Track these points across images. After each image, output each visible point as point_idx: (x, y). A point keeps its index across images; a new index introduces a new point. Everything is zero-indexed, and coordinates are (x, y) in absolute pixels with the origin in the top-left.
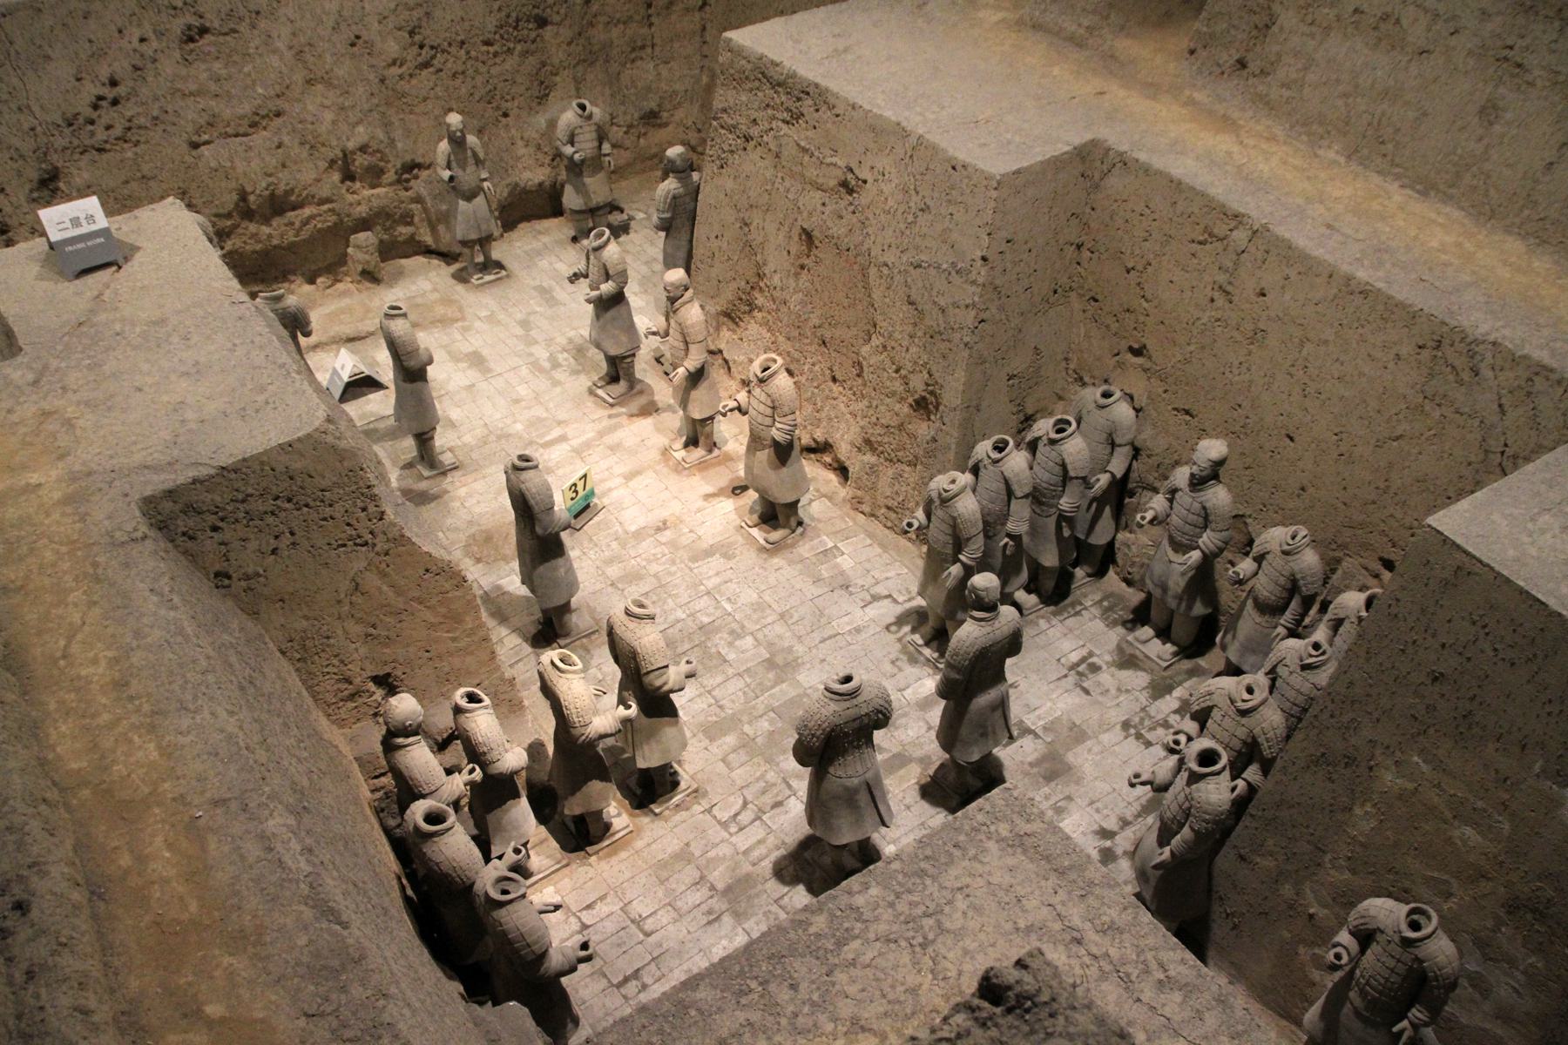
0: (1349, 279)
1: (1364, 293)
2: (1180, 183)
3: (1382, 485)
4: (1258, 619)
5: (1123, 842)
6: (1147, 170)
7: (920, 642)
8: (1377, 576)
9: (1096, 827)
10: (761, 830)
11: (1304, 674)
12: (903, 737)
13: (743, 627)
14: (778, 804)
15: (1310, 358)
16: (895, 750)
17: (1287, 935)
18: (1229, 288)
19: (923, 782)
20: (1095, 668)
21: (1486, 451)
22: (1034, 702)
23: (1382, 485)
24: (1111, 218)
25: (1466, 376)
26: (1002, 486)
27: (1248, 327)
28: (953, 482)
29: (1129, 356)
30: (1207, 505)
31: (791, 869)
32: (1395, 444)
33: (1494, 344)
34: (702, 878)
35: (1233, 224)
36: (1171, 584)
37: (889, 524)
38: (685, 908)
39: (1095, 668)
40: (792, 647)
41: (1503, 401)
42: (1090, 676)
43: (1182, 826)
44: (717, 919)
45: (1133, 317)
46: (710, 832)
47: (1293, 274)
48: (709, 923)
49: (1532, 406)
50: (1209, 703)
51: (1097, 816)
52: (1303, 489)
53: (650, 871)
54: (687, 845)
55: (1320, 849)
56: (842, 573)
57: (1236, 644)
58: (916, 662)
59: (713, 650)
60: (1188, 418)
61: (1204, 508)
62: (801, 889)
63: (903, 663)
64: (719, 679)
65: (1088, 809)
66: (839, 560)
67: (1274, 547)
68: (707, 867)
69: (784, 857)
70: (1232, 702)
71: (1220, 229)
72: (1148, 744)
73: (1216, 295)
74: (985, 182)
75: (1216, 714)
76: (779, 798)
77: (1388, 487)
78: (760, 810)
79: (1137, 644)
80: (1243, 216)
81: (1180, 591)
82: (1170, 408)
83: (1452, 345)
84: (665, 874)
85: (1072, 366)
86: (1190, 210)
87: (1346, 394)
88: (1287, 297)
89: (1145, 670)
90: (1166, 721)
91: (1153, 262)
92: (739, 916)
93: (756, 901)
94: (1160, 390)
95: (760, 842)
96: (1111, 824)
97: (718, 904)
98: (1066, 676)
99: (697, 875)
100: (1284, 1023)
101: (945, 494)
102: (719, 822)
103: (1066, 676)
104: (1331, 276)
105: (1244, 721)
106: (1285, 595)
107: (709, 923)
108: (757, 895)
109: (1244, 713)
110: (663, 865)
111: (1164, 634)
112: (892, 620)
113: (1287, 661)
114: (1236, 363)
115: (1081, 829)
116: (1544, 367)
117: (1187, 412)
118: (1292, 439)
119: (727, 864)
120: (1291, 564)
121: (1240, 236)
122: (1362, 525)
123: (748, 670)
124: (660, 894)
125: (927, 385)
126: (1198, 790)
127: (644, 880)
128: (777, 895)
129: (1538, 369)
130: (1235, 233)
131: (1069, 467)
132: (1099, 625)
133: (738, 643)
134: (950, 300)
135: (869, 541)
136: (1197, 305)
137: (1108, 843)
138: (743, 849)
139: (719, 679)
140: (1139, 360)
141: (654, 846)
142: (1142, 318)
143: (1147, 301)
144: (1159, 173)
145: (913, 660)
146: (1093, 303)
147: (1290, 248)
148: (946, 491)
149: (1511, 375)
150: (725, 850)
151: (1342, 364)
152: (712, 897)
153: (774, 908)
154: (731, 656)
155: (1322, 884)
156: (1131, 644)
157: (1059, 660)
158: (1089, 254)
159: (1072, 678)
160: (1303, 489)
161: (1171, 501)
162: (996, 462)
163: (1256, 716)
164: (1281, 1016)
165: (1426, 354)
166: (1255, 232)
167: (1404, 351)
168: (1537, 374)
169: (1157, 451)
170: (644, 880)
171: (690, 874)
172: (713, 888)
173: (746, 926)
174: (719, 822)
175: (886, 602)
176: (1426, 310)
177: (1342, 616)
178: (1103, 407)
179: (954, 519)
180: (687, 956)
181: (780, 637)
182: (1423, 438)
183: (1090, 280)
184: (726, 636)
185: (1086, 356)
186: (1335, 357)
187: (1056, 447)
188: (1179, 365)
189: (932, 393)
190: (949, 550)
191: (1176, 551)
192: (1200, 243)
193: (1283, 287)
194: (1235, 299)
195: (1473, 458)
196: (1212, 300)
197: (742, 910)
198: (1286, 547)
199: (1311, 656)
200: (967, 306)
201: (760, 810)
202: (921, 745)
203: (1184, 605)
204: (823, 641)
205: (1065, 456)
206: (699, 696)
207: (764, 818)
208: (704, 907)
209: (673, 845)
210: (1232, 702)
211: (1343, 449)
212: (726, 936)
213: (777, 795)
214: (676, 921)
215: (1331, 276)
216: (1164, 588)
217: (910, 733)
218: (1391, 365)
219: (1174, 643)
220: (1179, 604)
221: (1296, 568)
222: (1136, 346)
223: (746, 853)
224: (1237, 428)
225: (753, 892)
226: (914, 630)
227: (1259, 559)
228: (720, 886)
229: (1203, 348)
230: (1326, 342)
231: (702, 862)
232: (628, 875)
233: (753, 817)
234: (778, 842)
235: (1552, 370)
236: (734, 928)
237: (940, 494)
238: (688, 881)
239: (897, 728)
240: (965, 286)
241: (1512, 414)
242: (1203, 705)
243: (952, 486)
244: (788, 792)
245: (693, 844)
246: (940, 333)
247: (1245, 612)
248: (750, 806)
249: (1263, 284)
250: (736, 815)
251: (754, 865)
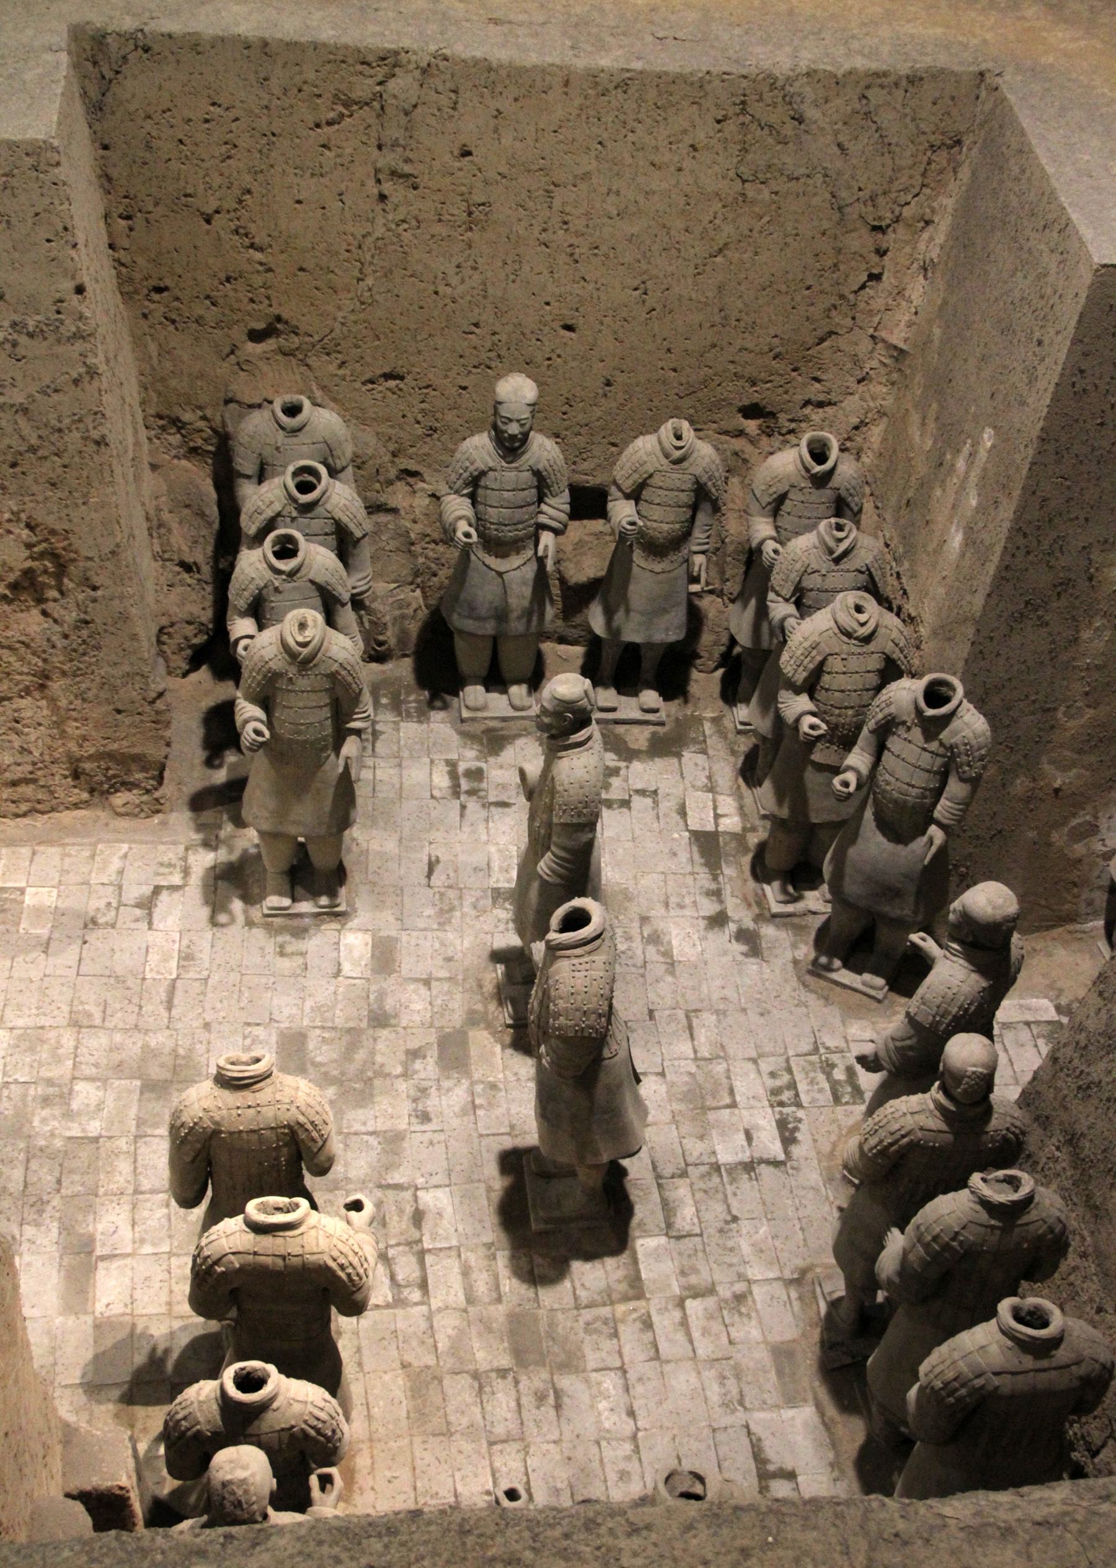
0: (593, 76)
1: (624, 85)
2: (265, 44)
3: (717, 319)
4: (658, 568)
5: (741, 915)
6: (194, 45)
7: (286, 902)
8: (740, 433)
9: (702, 924)
10: (448, 1262)
11: (841, 567)
12: (417, 1018)
13: (50, 1082)
14: (418, 1217)
15: (568, 209)
16: (433, 1038)
17: (1031, 834)
18: (407, 169)
19: (508, 1039)
20: (476, 775)
21: (840, 209)
22: (478, 859)
23: (717, 319)
24: (148, 147)
25: (789, 129)
26: (318, 601)
27: (458, 210)
28: (302, 626)
29: (251, 347)
30: (540, 467)
31: (538, 1260)
32: (719, 259)
33: (808, 74)
34: (476, 1376)
35: (380, 73)
36: (513, 601)
37: (24, 807)
38: (513, 1426)
39: (476, 775)
40: (145, 1047)
41: (841, 138)
42: (484, 785)
43: (938, 793)
44: (558, 1394)
45: (240, 285)
46: (401, 1325)
47: (505, 104)
48: (558, 1407)
49: (874, 127)
50: (819, 658)
51: (688, 912)
52: (608, 384)
53: (417, 1440)
54: (405, 1366)
55: (1049, 710)
56: (58, 913)
57: (635, 617)
58: (305, 930)
59: (58, 1143)
60: (392, 383)
61: (537, 473)
62: (577, 1266)
63: (294, 945)
64: (124, 1167)
65: (672, 913)
66: (29, 900)
67: (656, 462)
68: (461, 1360)
69: (513, 1257)
70: (848, 635)
71: (363, 88)
72: (626, 804)
73: (387, 187)
74: (30, 161)
75: (834, 664)
76: (409, 1210)
77: (725, 318)
78: (409, 1244)
79: (479, 714)
80: (396, 53)
81: (526, 603)
82: (358, 385)
83: (761, 100)
84: (436, 1422)
85: (152, 411)
86: (298, 79)
87: (635, 230)
88: (507, 140)
89: (519, 736)
90: (607, 768)
91: (255, 187)
92: (571, 1363)
93: (560, 1330)
94: (332, 368)
95: (466, 1272)
96: (710, 907)
97: (534, 1380)
98: (463, 807)
99: (465, 1380)
100: (1056, 932)
101: (305, 651)
102: (388, 1306)
103: (463, 807)
104: (567, 83)
105: (872, 647)
106: (690, 513)
107: (558, 1407)
108: (552, 1325)
109: (867, 639)
110: (419, 1416)
111: (495, 681)
112: (205, 912)
113: (815, 566)
114: (451, 270)
115: (696, 937)
116: (876, 74)
117: (388, 376)
118: (569, 328)
119: (474, 1331)
120: (690, 471)
121: (402, 85)
122: (705, 383)
123: (140, 1122)
124: (467, 1447)
125: (29, 546)
126: (955, 733)
127: (428, 1457)
128: (569, 1301)
129: (869, 80)
130: (391, 84)
131: (352, 527)
132: (410, 729)
133: (75, 1105)
134: (33, 389)
135: (25, 851)
136: (357, 216)
137: (732, 927)
138: (461, 1298)
139: (124, 1167)
140: (271, 344)
141: (375, 1411)
142: (258, 280)
143: (260, 249)
144: (221, 42)
145: (300, 933)
146: (156, 297)
147: (490, 69)
148: (304, 645)
149: (838, 102)
150: (447, 1326)
151: (618, 193)
152: (517, 1382)
153: (587, 1315)
154: (94, 1127)
155: (1062, 746)
156: (473, 719)
157: (432, 797)
158: (123, 223)
159: (472, 805)
160: (608, 384)
161: (473, 497)
162: (292, 574)
163: (882, 631)
164: (1048, 928)
165: (731, 127)
166: (424, 71)
167: (701, 136)
168: (868, 87)
169: (370, 452)
170: (428, 1457)
171: (460, 1390)
172: (502, 1373)
173: (591, 1365)
174: (388, 1306)
175: (164, 896)
176: (715, 70)
177: (782, 490)
178: (300, 430)
179: (333, 676)
180: (596, 1465)
181: (114, 1048)
182: (755, 234)
183: (141, 261)
184: (45, 1113)
185: (173, 383)
186: (604, 190)
187: (319, 510)
188: (353, 317)
189: (42, 556)
190: (329, 731)
191: (503, 556)
192: (330, 123)
193: (496, 130)
194: (422, 181)
195: (826, 225)
196: (383, 197)
197: (563, 1356)
198: (677, 454)
199: (840, 540)
200: (76, 382)
201: (409, 1244)
202: (445, 1007)
203: (535, 619)
204: (170, 1005)
205: (338, 514)
206: (134, 1206)
207: (426, 1246)
208: (527, 1401)
209: (396, 1385)
210: (848, 635)
211: (651, 301)
212: (593, 1397)
213: (401, 1212)
214: (526, 1450)
215: (567, 83)
216: (501, 615)
217: (418, 1006)
218: (687, 164)
219: (518, 682)
220: (529, 621)
221: (698, 471)
222: (260, 325)
223: (470, 1300)
224: (484, 355)
225: (543, 1326)
226: (249, 899)
227: (635, 495)
228: (506, 1361)
229: (388, 273)
230: (586, 176)
231: (449, 1363)
232: (405, 1475)
233: (413, 1260)
234: (482, 1252)
235: (885, 74)
236: (587, 1381)
237: (292, 655)
238: (469, 1397)
239: (396, 1016)
240: (59, 349)
241: (853, 148)
242: (811, 666)
243: (309, 633)
244: (407, 1195)
245: (408, 1357)
246: (33, 449)
247: (635, 569)
248: (391, 1253)
249: (463, 139)
250: (393, 1278)
251: (499, 1300)
